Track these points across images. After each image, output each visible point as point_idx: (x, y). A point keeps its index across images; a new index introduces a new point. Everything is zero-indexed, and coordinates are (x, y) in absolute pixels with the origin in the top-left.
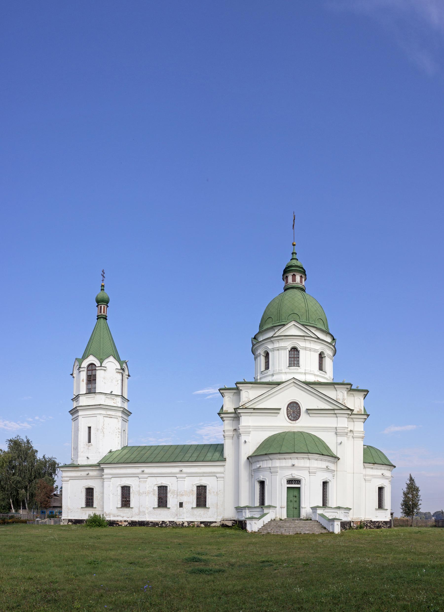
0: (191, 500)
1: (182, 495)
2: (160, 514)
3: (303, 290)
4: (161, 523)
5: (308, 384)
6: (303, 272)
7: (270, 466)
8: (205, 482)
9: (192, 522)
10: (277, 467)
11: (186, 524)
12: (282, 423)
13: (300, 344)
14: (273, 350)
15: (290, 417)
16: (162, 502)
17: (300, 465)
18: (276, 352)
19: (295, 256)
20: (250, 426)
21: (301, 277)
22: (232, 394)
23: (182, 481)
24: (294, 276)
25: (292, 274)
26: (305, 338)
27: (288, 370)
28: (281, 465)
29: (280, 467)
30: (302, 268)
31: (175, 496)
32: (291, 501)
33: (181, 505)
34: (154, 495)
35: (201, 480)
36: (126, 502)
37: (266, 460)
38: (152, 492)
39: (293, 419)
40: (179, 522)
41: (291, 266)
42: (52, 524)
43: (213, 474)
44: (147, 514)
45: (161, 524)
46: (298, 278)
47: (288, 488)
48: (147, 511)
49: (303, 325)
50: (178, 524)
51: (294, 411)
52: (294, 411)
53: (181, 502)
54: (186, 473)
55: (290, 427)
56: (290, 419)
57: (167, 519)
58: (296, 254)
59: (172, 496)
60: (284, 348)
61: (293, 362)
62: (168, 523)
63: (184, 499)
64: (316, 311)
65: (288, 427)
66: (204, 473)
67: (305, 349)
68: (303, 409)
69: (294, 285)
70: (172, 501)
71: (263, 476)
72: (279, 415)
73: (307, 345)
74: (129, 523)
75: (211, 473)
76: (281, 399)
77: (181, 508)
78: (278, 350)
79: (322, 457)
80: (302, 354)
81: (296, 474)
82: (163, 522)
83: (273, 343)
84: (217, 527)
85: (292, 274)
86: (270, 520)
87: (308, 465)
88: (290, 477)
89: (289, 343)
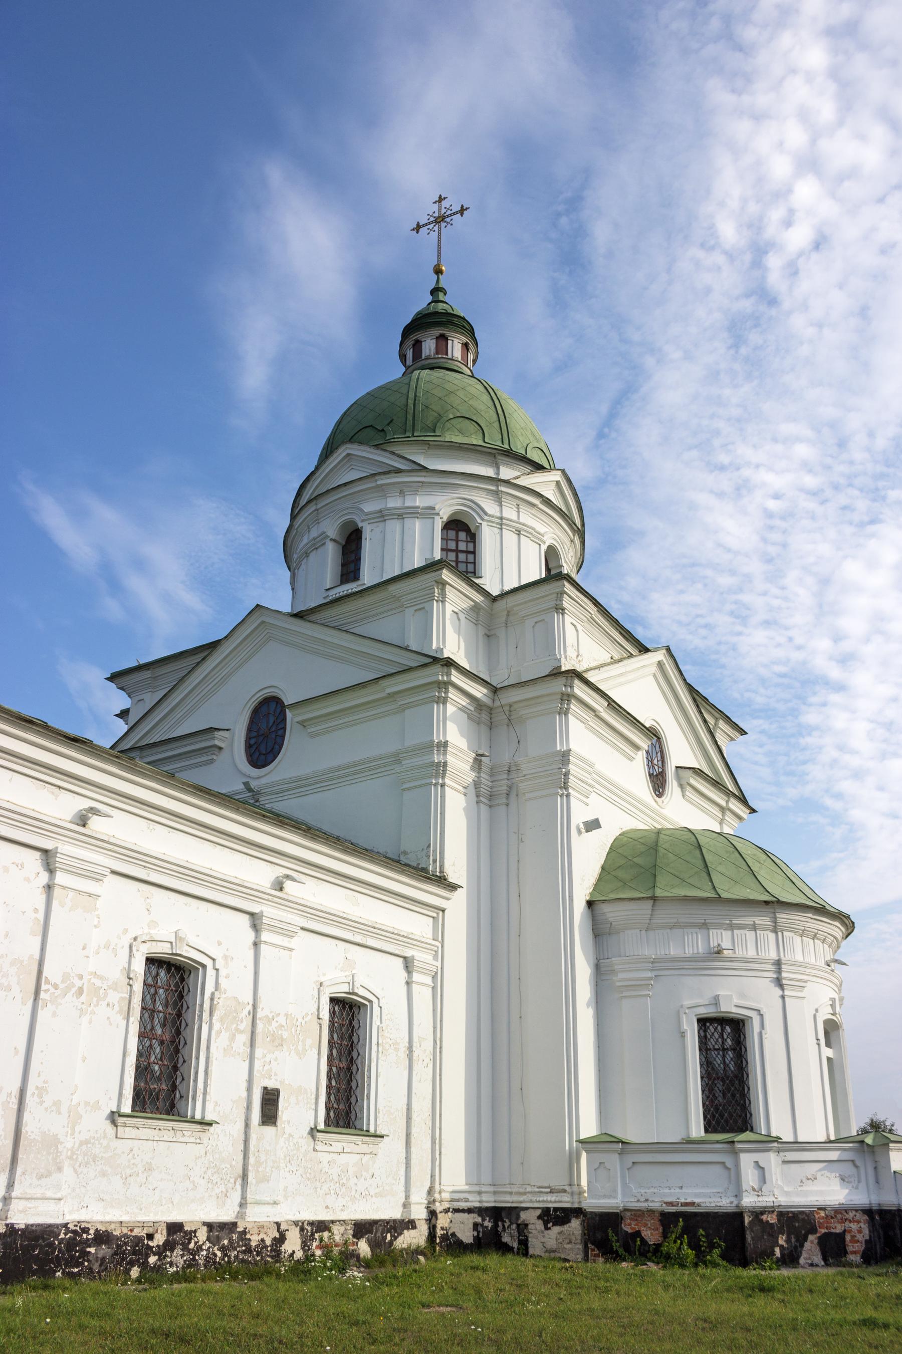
0: (303, 1076)
1: (278, 1042)
2: (149, 1168)
4: (160, 1239)
7: (773, 956)
9: (322, 1226)
11: (293, 1245)
14: (501, 523)
19: (441, 296)
20: (592, 766)
22: (466, 604)
31: (244, 1038)
37: (754, 928)
38: (115, 987)
40: (261, 1228)
41: (436, 313)
44: (67, 1170)
45: (161, 1252)
47: (829, 1059)
48: (69, 1143)
50: (254, 1240)
53: (271, 1085)
57: (198, 1210)
59: (225, 1035)
60: (537, 538)
62: (202, 1235)
66: (374, 930)
71: (742, 995)
75: (396, 936)
77: (269, 1130)
78: (519, 533)
82: (174, 1228)
84: (418, 1251)
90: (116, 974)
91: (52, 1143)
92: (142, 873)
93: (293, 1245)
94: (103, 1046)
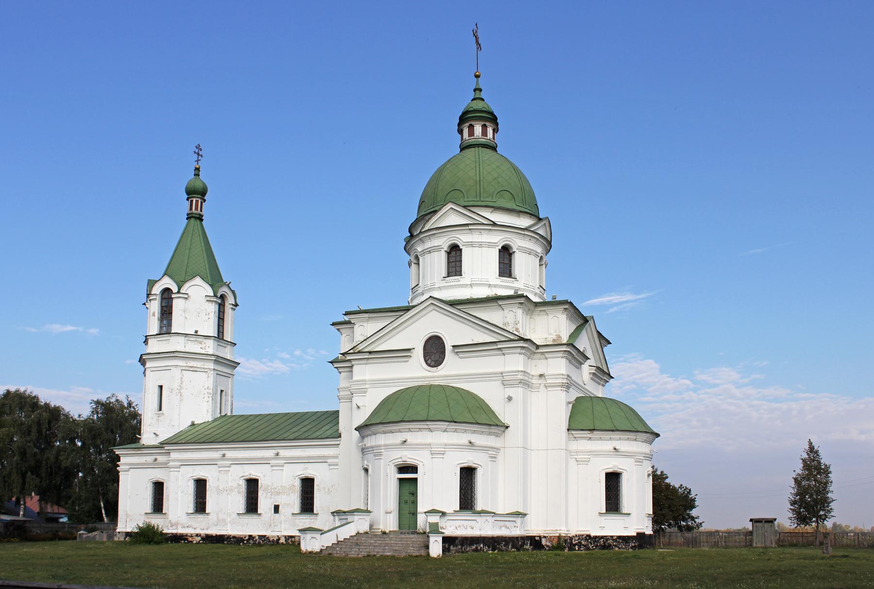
0: (292, 501)
1: (278, 493)
3: (494, 148)
5: (453, 304)
6: (494, 120)
8: (311, 472)
10: (380, 446)
11: (283, 540)
12: (415, 372)
13: (462, 238)
15: (429, 362)
16: (252, 506)
17: (415, 441)
18: (427, 256)
21: (484, 127)
23: (279, 470)
24: (471, 127)
25: (468, 124)
26: (470, 227)
27: (443, 284)
28: (388, 442)
29: (385, 445)
30: (492, 114)
32: (406, 502)
33: (277, 509)
34: (239, 493)
35: (307, 469)
36: (200, 506)
39: (433, 363)
42: (105, 539)
43: (322, 460)
44: (229, 525)
46: (478, 129)
49: (465, 207)
51: (434, 350)
52: (434, 350)
54: (284, 458)
55: (428, 377)
56: (429, 365)
57: (256, 533)
58: (481, 90)
59: (265, 495)
60: (438, 249)
61: (454, 269)
63: (280, 500)
64: (495, 179)
65: (424, 377)
67: (471, 244)
68: (448, 348)
69: (472, 141)
70: (264, 503)
72: (410, 360)
73: (475, 237)
74: (203, 539)
75: (319, 457)
76: (413, 335)
77: (277, 515)
79: (454, 426)
80: (467, 255)
81: (408, 457)
82: (250, 536)
83: (423, 242)
85: (468, 124)
86: (354, 534)
87: (429, 441)
88: (399, 462)
89: (445, 239)
90: (236, 485)
91: (224, 520)
92: (238, 462)
93: (283, 540)
94: (240, 502)
